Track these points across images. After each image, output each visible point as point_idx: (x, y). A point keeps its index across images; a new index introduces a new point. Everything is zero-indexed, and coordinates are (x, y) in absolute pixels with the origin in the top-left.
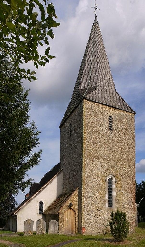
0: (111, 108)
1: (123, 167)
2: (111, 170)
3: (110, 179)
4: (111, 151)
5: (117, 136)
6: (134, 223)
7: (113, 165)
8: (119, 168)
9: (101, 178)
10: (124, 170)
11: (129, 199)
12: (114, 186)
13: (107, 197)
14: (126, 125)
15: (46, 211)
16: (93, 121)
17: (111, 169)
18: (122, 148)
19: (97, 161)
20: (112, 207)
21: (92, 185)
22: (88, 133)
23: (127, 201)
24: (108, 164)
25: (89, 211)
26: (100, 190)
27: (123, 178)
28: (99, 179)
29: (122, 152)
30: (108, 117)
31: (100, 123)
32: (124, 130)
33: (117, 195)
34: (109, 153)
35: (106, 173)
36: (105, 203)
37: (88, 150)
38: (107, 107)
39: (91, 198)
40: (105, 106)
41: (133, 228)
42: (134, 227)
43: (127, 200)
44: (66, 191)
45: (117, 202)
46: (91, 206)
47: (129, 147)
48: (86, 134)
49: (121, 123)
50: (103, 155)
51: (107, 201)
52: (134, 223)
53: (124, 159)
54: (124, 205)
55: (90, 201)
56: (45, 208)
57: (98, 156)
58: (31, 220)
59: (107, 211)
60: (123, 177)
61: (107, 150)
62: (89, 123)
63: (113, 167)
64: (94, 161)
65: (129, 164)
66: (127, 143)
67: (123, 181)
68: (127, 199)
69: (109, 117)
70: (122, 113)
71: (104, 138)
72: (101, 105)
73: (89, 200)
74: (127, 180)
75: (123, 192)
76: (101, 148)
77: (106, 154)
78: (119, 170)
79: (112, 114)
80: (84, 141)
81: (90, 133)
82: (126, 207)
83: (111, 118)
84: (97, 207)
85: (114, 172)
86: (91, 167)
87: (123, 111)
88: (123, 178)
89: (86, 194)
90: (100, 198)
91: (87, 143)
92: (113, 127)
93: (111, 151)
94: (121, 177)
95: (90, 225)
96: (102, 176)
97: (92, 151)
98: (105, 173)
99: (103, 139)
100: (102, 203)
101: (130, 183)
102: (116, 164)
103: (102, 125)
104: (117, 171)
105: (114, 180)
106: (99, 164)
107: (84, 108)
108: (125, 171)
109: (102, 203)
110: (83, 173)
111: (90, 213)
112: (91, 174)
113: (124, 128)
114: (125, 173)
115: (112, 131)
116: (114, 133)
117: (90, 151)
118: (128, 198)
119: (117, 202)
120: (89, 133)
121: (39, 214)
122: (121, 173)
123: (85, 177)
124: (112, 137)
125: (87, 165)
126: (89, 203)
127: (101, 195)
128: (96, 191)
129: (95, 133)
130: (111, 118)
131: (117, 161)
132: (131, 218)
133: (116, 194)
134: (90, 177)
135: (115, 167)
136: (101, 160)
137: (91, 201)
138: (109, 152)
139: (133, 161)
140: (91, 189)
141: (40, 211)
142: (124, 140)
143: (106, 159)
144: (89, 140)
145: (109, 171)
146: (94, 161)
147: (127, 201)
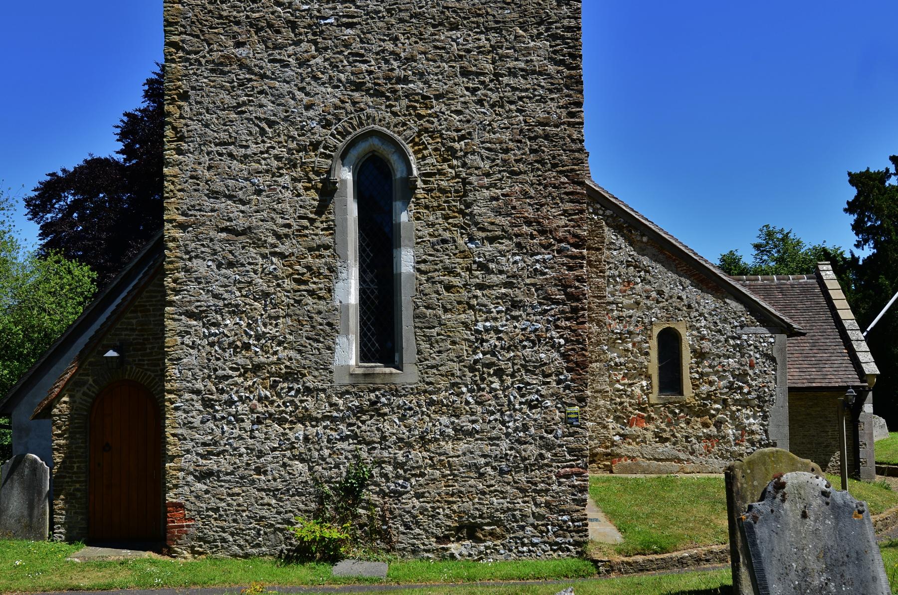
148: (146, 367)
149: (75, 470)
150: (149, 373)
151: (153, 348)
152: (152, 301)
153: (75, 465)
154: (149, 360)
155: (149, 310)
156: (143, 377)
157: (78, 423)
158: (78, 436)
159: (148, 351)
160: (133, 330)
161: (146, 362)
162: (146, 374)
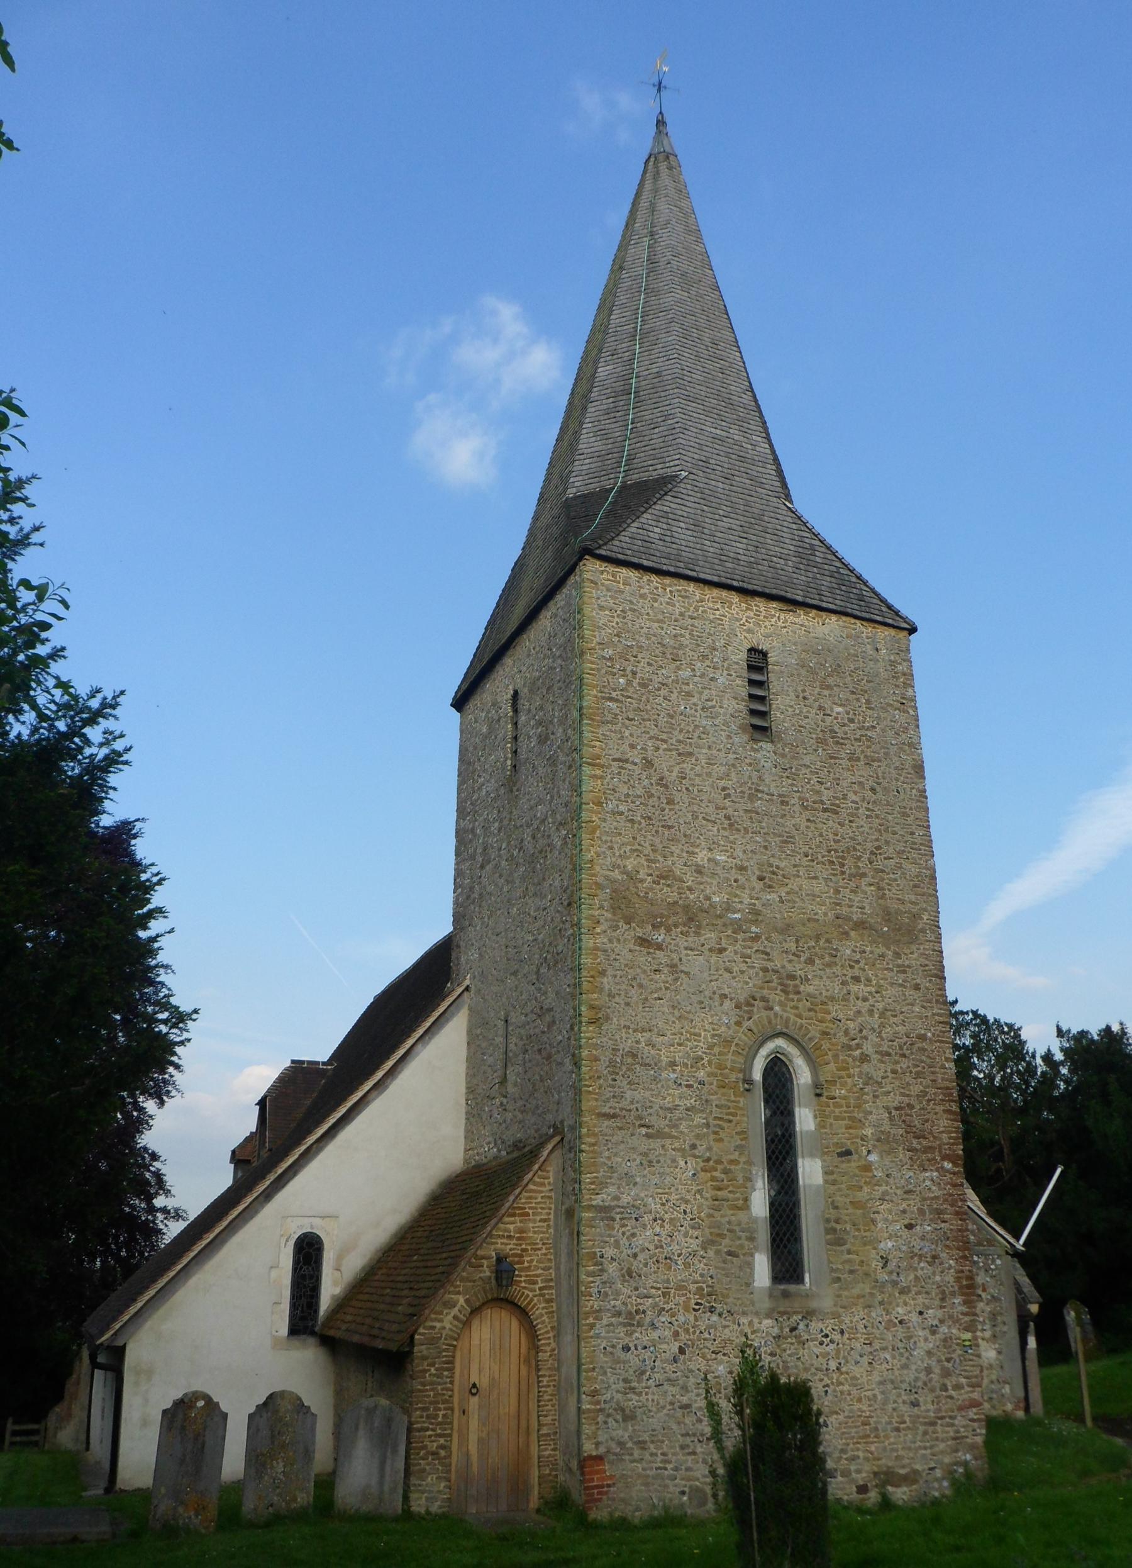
0: (760, 604)
1: (857, 979)
2: (781, 1004)
3: (777, 1069)
4: (774, 873)
5: (804, 771)
7: (789, 967)
8: (836, 989)
9: (710, 1062)
10: (865, 1000)
11: (921, 1212)
12: (805, 1119)
13: (759, 1204)
14: (858, 700)
15: (342, 1305)
16: (644, 685)
17: (776, 997)
18: (842, 846)
19: (682, 942)
20: (800, 1280)
21: (653, 1120)
22: (614, 760)
24: (758, 962)
25: (632, 1319)
26: (709, 1149)
27: (864, 1058)
28: (701, 1074)
29: (843, 873)
30: (740, 657)
31: (689, 694)
32: (846, 733)
33: (834, 1183)
34: (759, 885)
35: (746, 1024)
36: (752, 1255)
37: (616, 875)
38: (735, 598)
39: (647, 1218)
40: (716, 592)
41: (972, 1447)
42: (979, 1440)
43: (906, 1222)
44: (488, 1151)
45: (835, 1238)
46: (650, 1282)
47: (887, 843)
48: (602, 766)
49: (826, 692)
50: (716, 899)
51: (763, 1235)
53: (860, 925)
54: (892, 1265)
55: (639, 1241)
56: (331, 1288)
57: (687, 908)
58: (208, 1399)
59: (768, 1316)
60: (868, 1048)
61: (742, 869)
62: (620, 697)
63: (788, 983)
64: (659, 947)
65: (897, 955)
66: (877, 816)
67: (869, 1080)
68: (904, 1212)
69: (744, 655)
70: (826, 629)
71: (724, 789)
72: (691, 587)
73: (633, 1235)
74: (894, 1072)
75: (873, 1158)
76: (702, 857)
77: (736, 896)
78: (832, 999)
79: (767, 636)
80: (592, 811)
81: (627, 761)
82: (906, 1279)
83: (757, 660)
84: (693, 1287)
85: (800, 1016)
86: (641, 986)
87: (834, 618)
88: (864, 1058)
89: (612, 1189)
90: (710, 1216)
91: (611, 824)
92: (776, 714)
93: (774, 873)
94: (850, 1048)
95: (646, 1437)
96: (716, 1050)
97: (641, 876)
98: (738, 1024)
99: (718, 797)
100: (730, 1253)
101: (916, 1089)
102: (810, 961)
103: (703, 709)
104: (818, 1004)
105: (802, 1075)
106: (695, 963)
107: (587, 610)
108: (880, 1006)
109: (730, 1253)
110: (588, 1032)
111: (641, 1336)
112: (643, 1037)
113: (851, 721)
114: (875, 1021)
115: (772, 742)
116: (783, 756)
117: (632, 877)
118: (914, 1204)
119: (840, 1242)
120: (619, 760)
121: (284, 1331)
122: (851, 1025)
123: (597, 1059)
124: (773, 784)
125: (610, 972)
126: (635, 1256)
127: (719, 1189)
128: (682, 1163)
129: (665, 763)
130: (757, 660)
131: (818, 938)
132: (948, 1360)
133: (826, 1181)
134: (635, 1056)
135: (807, 980)
136: (710, 936)
137: (646, 1237)
138: (761, 879)
139: (923, 931)
140: (644, 1145)
141: (294, 1306)
142: (855, 793)
143: (738, 927)
144: (622, 808)
145: (764, 1013)
146: (659, 947)
147: (910, 1227)
148: (523, 1284)
149: (440, 1419)
150: (526, 1292)
151: (532, 1261)
152: (531, 1203)
153: (441, 1413)
154: (527, 1276)
155: (528, 1215)
156: (522, 1296)
157: (446, 1356)
158: (446, 1373)
159: (526, 1264)
160: (509, 1237)
161: (523, 1279)
162: (523, 1293)
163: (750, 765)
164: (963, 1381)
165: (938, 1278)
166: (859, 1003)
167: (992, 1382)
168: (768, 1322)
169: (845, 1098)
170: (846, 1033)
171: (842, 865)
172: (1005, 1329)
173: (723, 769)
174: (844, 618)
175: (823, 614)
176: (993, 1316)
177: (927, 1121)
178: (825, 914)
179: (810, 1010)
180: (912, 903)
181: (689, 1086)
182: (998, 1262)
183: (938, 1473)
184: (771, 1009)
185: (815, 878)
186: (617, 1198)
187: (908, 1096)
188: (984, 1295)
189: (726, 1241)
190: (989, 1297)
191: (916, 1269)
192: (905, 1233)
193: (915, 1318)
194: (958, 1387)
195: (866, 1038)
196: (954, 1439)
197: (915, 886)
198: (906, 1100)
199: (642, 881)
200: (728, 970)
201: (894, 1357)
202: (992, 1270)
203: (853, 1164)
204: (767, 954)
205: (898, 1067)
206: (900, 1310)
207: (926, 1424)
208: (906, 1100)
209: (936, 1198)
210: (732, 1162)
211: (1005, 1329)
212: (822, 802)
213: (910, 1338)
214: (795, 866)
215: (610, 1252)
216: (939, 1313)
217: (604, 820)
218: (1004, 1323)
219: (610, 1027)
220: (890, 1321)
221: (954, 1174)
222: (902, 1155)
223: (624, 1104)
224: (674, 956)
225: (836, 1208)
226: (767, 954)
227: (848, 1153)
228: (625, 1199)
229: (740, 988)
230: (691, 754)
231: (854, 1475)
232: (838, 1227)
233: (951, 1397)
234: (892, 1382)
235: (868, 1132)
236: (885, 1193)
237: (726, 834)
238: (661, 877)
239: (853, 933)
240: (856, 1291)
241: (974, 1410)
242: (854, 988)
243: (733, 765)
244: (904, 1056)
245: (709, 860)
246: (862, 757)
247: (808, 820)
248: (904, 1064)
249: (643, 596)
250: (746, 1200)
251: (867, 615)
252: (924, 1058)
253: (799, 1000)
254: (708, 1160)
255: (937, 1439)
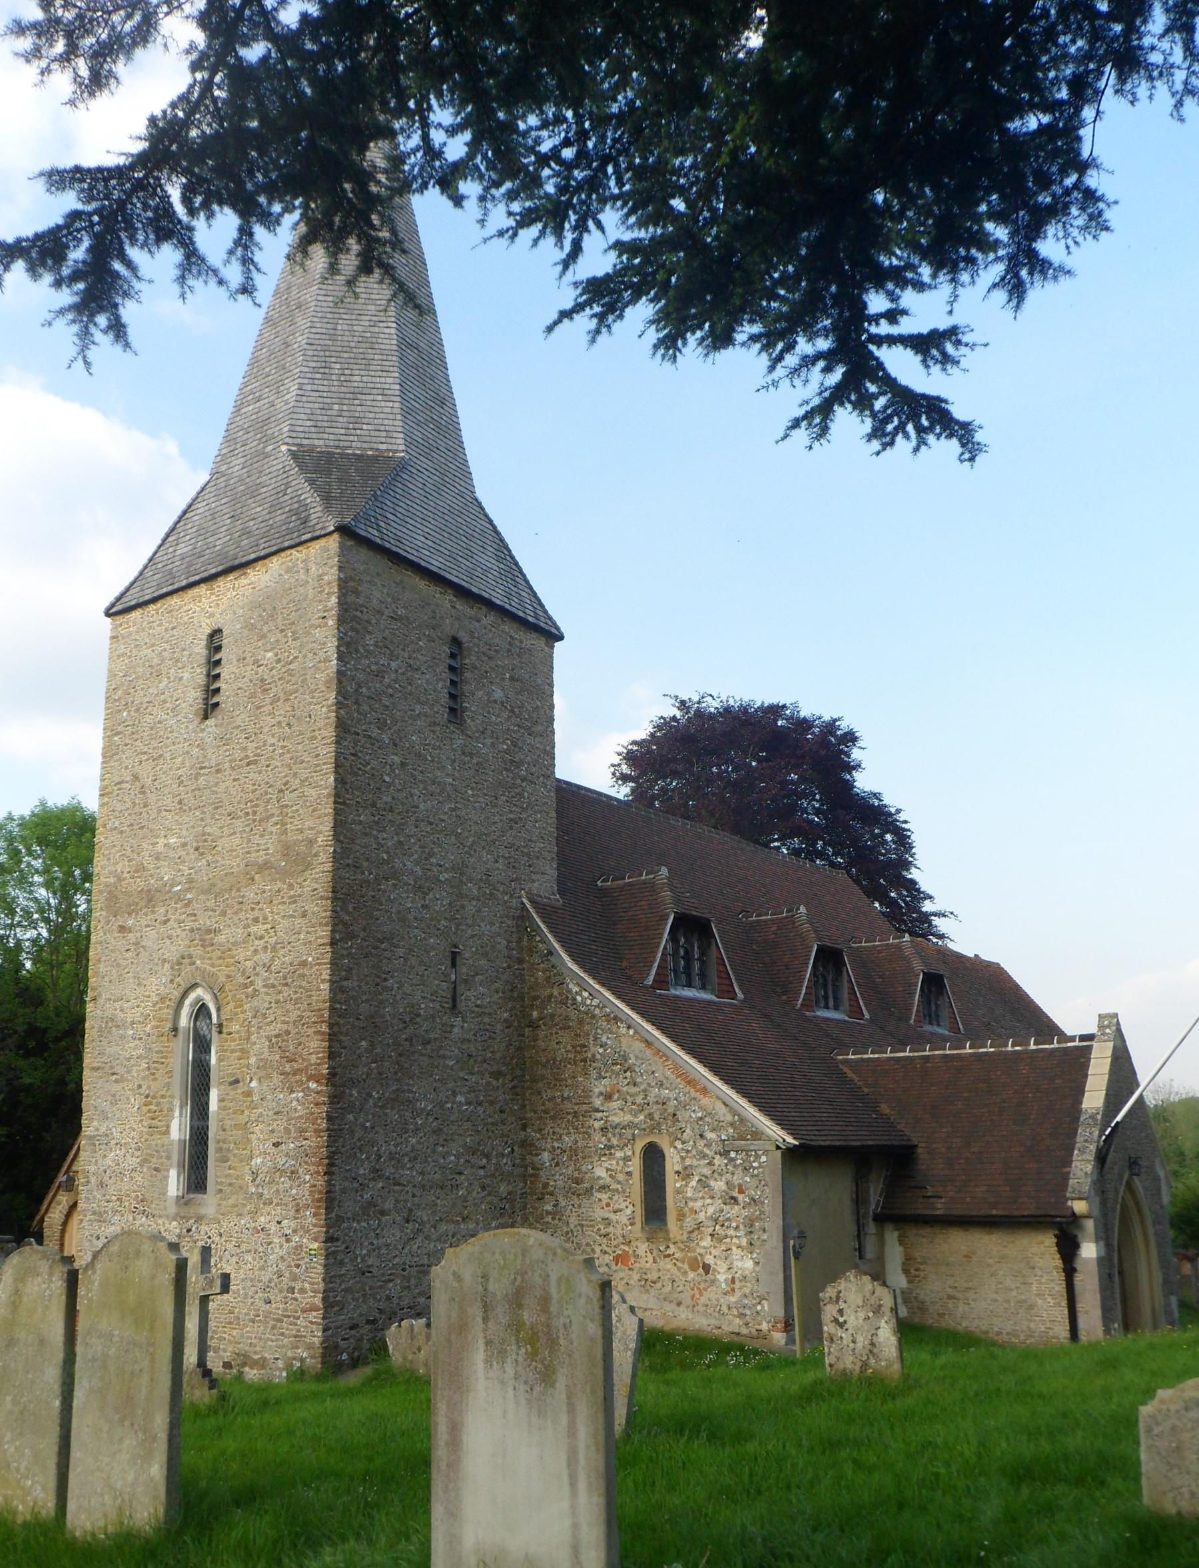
0: (221, 583)
1: (256, 920)
2: (202, 958)
4: (205, 841)
5: (236, 732)
6: (313, 1308)
10: (261, 938)
11: (287, 1131)
14: (286, 636)
17: (197, 951)
23: (276, 1145)
26: (149, 1088)
38: (202, 589)
41: (310, 1347)
42: (317, 1341)
43: (275, 1141)
49: (260, 644)
52: (313, 1308)
59: (174, 1219)
63: (205, 937)
68: (272, 1131)
74: (277, 1002)
75: (254, 1084)
78: (235, 944)
84: (133, 1195)
85: (213, 966)
87: (275, 559)
97: (126, 875)
98: (172, 981)
101: (294, 1016)
109: (156, 1169)
112: (118, 1005)
113: (279, 661)
118: (280, 1125)
120: (119, 783)
132: (298, 1266)
138: (197, 849)
139: (316, 855)
142: (273, 736)
147: (276, 1145)
163: (198, 746)
164: (307, 1285)
165: (294, 1191)
166: (257, 942)
167: (746, 1296)
168: (174, 1223)
169: (238, 1032)
170: (243, 973)
171: (255, 813)
172: (765, 1237)
173: (180, 759)
174: (283, 554)
175: (266, 561)
176: (750, 1223)
177: (300, 1044)
178: (238, 866)
179: (220, 958)
180: (310, 829)
181: (140, 1039)
182: (764, 1159)
183: (280, 1364)
184: (194, 963)
185: (234, 833)
186: (97, 1130)
187: (287, 1022)
188: (740, 1197)
189: (154, 1160)
190: (747, 1200)
191: (278, 1183)
192: (274, 1150)
193: (273, 1227)
194: (303, 1291)
195: (257, 974)
196: (296, 1336)
197: (314, 811)
198: (285, 1026)
199: (125, 879)
200: (170, 938)
201: (254, 1259)
202: (754, 1168)
203: (239, 1091)
204: (195, 915)
205: (280, 997)
206: (262, 1219)
207: (274, 1319)
208: (285, 1026)
209: (301, 1117)
210: (163, 1097)
211: (765, 1237)
212: (247, 757)
213: (270, 1243)
214: (221, 828)
215: (92, 1168)
216: (293, 1224)
217: (106, 838)
218: (764, 1230)
219: (101, 1001)
220: (255, 1228)
221: (318, 1093)
222: (277, 1079)
223: (105, 1059)
224: (139, 935)
225: (224, 1130)
226: (195, 915)
227: (237, 1081)
228: (103, 1129)
229: (172, 951)
230: (161, 756)
231: (221, 1353)
232: (225, 1146)
233: (296, 1300)
234: (252, 1280)
235: (253, 1060)
236: (260, 1115)
237: (177, 817)
238: (136, 871)
239: (257, 877)
240: (231, 1201)
241: (314, 1313)
242: (253, 929)
243: (188, 752)
244: (286, 985)
245: (165, 845)
246: (282, 695)
247: (235, 780)
248: (287, 992)
249: (143, 630)
250: (168, 1127)
251: (297, 540)
252: (304, 984)
253: (213, 951)
254: (147, 1097)
255: (282, 1334)
